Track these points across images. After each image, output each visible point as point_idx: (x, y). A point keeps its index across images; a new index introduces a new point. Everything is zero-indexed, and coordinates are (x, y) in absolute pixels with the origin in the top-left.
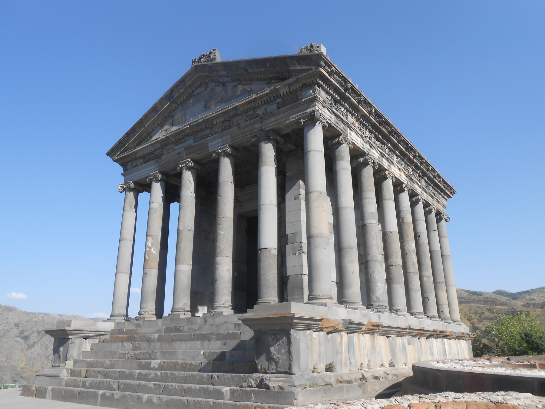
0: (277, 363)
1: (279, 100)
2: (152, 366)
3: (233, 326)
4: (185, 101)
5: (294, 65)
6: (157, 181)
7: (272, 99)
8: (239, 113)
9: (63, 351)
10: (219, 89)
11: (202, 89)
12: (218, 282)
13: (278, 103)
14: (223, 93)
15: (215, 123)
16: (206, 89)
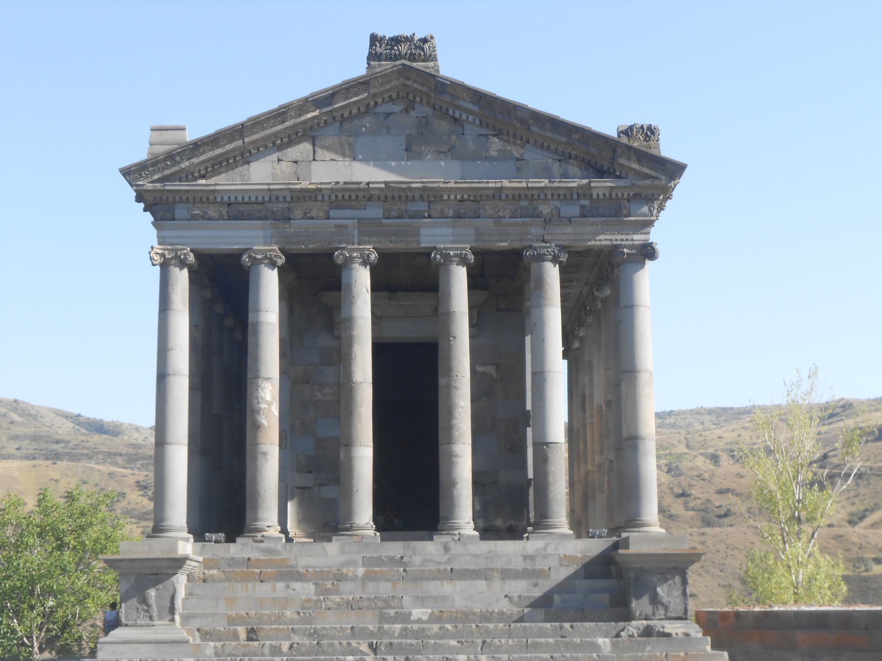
0: (666, 608)
1: (586, 202)
2: (412, 618)
3: (521, 559)
4: (351, 117)
5: (629, 159)
6: (272, 264)
7: (575, 196)
8: (503, 197)
9: (159, 597)
10: (442, 126)
11: (397, 108)
12: (458, 486)
13: (581, 206)
14: (454, 137)
15: (446, 197)
16: (406, 111)
